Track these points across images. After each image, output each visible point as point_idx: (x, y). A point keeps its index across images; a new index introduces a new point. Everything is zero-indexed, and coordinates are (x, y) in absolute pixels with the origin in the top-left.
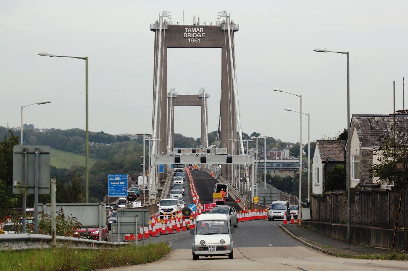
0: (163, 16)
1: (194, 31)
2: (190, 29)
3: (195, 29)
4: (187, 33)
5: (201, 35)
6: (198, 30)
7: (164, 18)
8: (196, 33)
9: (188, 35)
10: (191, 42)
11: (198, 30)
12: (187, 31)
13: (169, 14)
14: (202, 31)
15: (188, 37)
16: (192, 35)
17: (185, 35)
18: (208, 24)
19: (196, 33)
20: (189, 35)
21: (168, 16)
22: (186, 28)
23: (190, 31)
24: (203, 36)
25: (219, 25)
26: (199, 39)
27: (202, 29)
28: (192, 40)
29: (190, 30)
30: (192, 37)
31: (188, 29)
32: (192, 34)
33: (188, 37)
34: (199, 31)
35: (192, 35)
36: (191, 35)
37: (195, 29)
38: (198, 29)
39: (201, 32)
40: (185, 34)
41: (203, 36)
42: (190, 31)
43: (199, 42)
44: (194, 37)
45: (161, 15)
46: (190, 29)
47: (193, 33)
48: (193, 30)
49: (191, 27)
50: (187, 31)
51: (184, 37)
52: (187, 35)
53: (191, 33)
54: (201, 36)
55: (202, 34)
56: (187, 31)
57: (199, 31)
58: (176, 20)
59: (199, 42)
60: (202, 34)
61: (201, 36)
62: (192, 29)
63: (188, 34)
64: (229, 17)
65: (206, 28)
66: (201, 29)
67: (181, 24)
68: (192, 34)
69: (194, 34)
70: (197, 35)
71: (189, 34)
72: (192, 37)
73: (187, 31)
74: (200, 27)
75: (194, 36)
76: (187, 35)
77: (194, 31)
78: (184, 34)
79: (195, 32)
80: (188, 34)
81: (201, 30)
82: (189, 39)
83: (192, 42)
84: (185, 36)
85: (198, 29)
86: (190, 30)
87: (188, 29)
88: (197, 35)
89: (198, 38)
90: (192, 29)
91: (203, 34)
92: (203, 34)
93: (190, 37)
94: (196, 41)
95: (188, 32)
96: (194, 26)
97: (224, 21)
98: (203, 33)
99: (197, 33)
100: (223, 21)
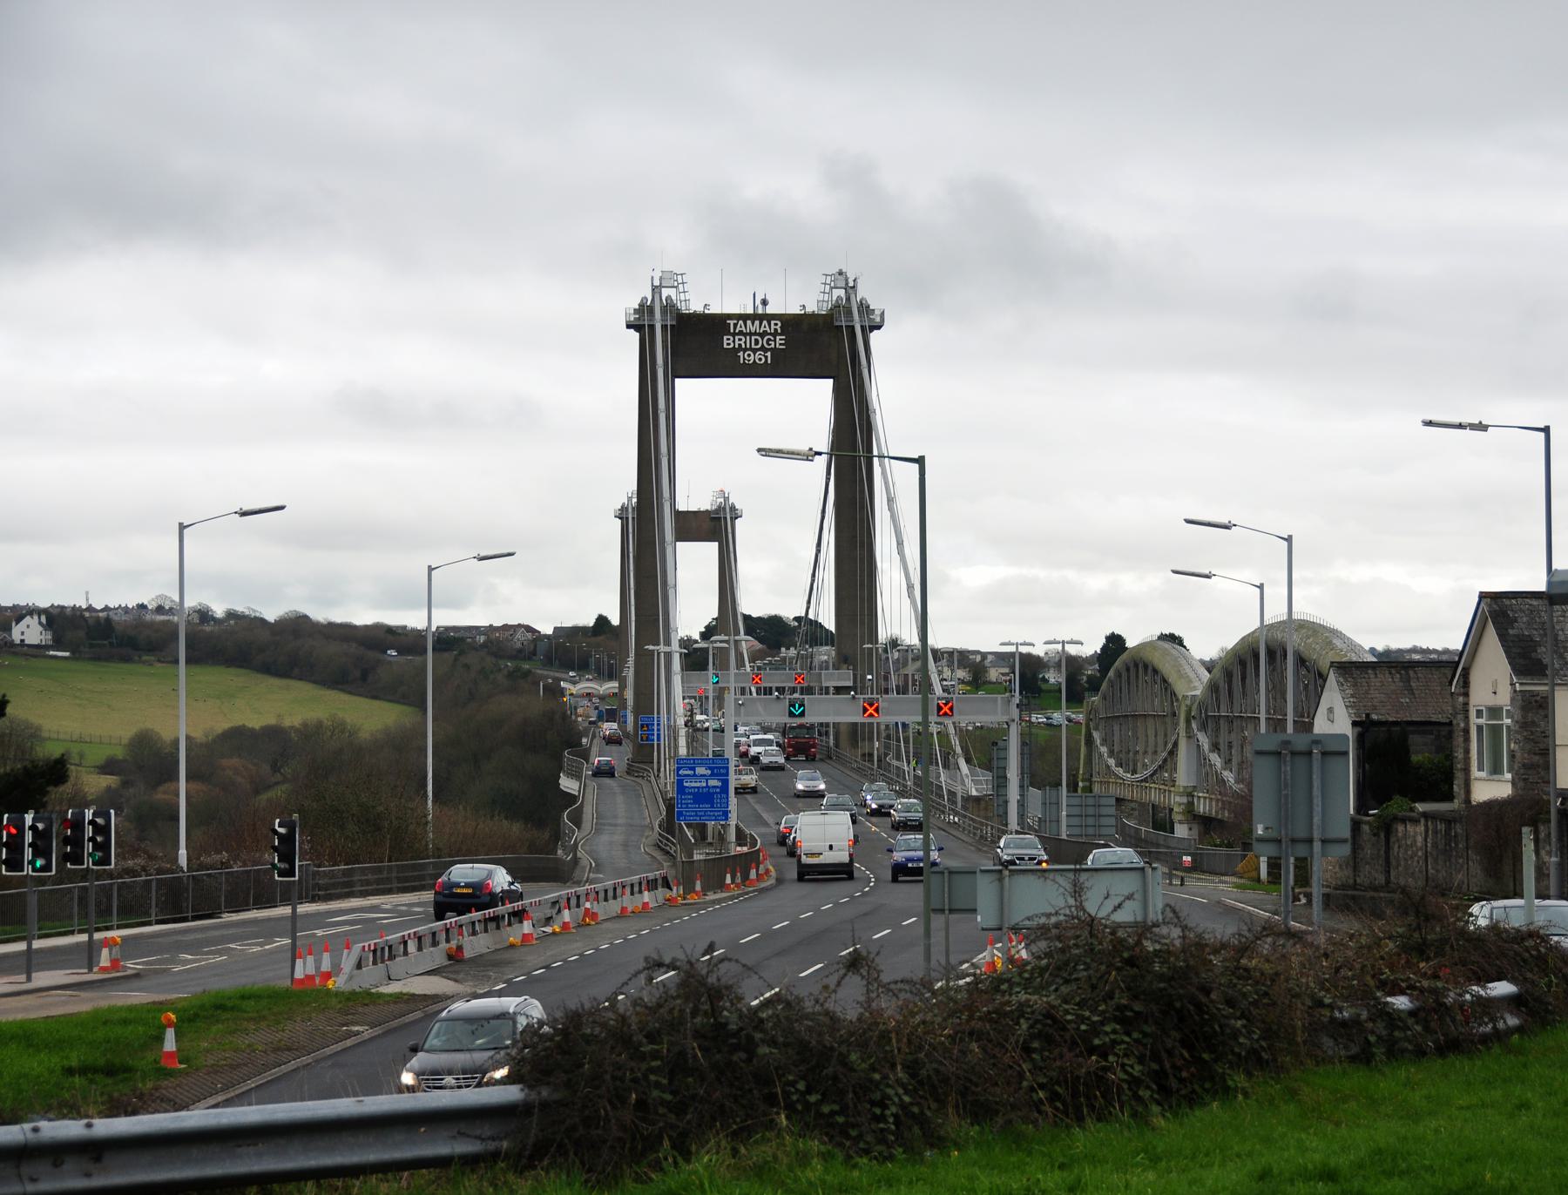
0: (661, 286)
4: (734, 335)
7: (665, 292)
17: (728, 342)
18: (794, 309)
20: (740, 341)
22: (732, 323)
39: (775, 334)
45: (657, 283)
47: (751, 334)
48: (752, 327)
49: (744, 317)
53: (745, 335)
58: (698, 299)
67: (715, 309)
70: (763, 342)
74: (770, 318)
88: (763, 342)
89: (766, 350)
99: (762, 335)
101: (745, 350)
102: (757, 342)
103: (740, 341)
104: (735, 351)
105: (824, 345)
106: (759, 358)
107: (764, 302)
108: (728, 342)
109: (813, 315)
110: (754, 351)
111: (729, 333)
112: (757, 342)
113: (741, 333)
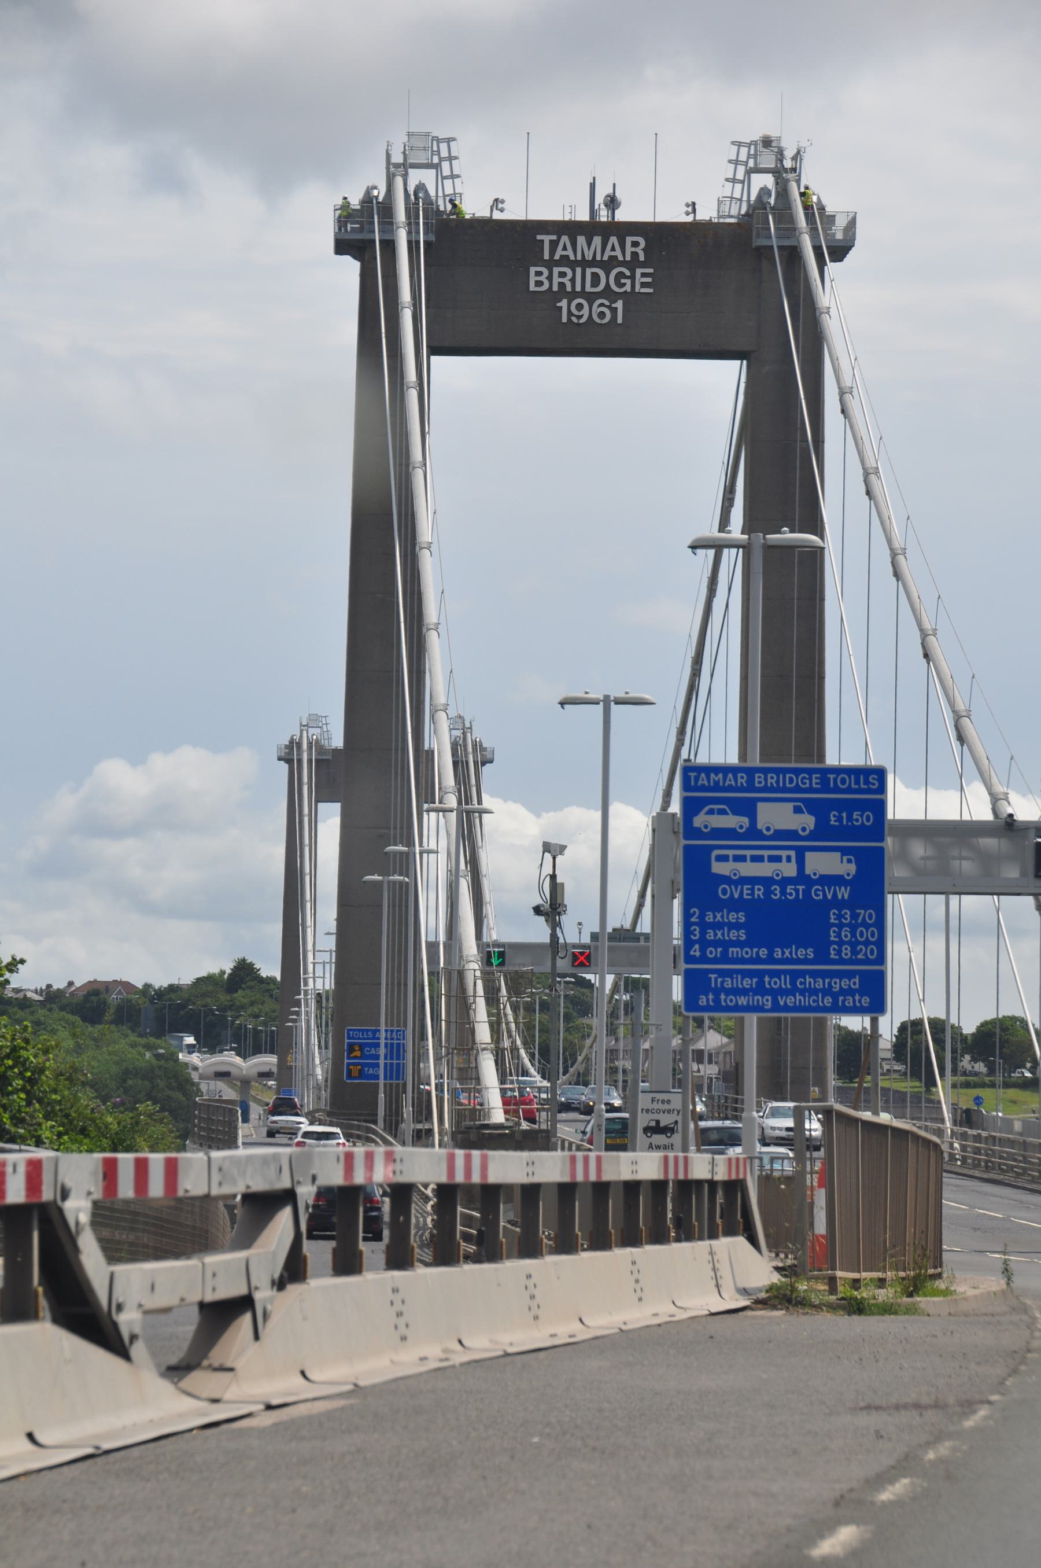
0: (405, 166)
1: (589, 257)
2: (565, 239)
3: (597, 240)
4: (550, 264)
5: (633, 277)
6: (613, 249)
8: (601, 264)
9: (556, 279)
10: (574, 319)
11: (613, 249)
12: (546, 257)
13: (444, 153)
14: (635, 255)
15: (555, 288)
16: (580, 279)
17: (537, 279)
18: (673, 213)
19: (601, 264)
20: (560, 278)
21: (436, 160)
22: (546, 239)
23: (570, 252)
24: (643, 285)
25: (735, 212)
26: (619, 305)
27: (635, 244)
28: (580, 307)
29: (565, 248)
30: (578, 288)
31: (554, 245)
32: (579, 270)
33: (555, 288)
34: (618, 253)
35: (580, 279)
36: (573, 281)
37: (597, 240)
38: (613, 240)
39: (633, 263)
40: (539, 274)
41: (643, 285)
42: (570, 252)
43: (620, 320)
44: (588, 288)
45: (397, 158)
46: (565, 239)
47: (584, 264)
49: (570, 229)
50: (546, 257)
51: (532, 287)
52: (550, 278)
53: (573, 265)
54: (628, 282)
55: (639, 271)
56: (552, 252)
57: (618, 253)
59: (620, 320)
60: (639, 271)
61: (628, 282)
62: (581, 240)
63: (556, 270)
64: (794, 170)
65: (661, 237)
66: (629, 240)
67: (514, 212)
68: (579, 270)
69: (589, 271)
71: (562, 275)
72: (578, 288)
73: (552, 252)
75: (592, 286)
76: (550, 278)
77: (589, 257)
78: (533, 270)
79: (593, 263)
80: (556, 270)
81: (629, 249)
82: (564, 304)
83: (579, 317)
84: (539, 284)
85: (613, 240)
86: (565, 248)
87: (554, 245)
90: (581, 240)
91: (643, 275)
92: (643, 275)
93: (569, 289)
94: (602, 315)
95: (557, 257)
96: (591, 229)
97: (764, 191)
98: (643, 265)
100: (759, 197)
101: (573, 295)
102: (596, 278)
103: (560, 278)
104: (554, 296)
105: (735, 286)
106: (596, 311)
107: (612, 202)
108: (537, 279)
109: (708, 225)
110: (591, 298)
111: (540, 261)
112: (596, 278)
113: (565, 261)
